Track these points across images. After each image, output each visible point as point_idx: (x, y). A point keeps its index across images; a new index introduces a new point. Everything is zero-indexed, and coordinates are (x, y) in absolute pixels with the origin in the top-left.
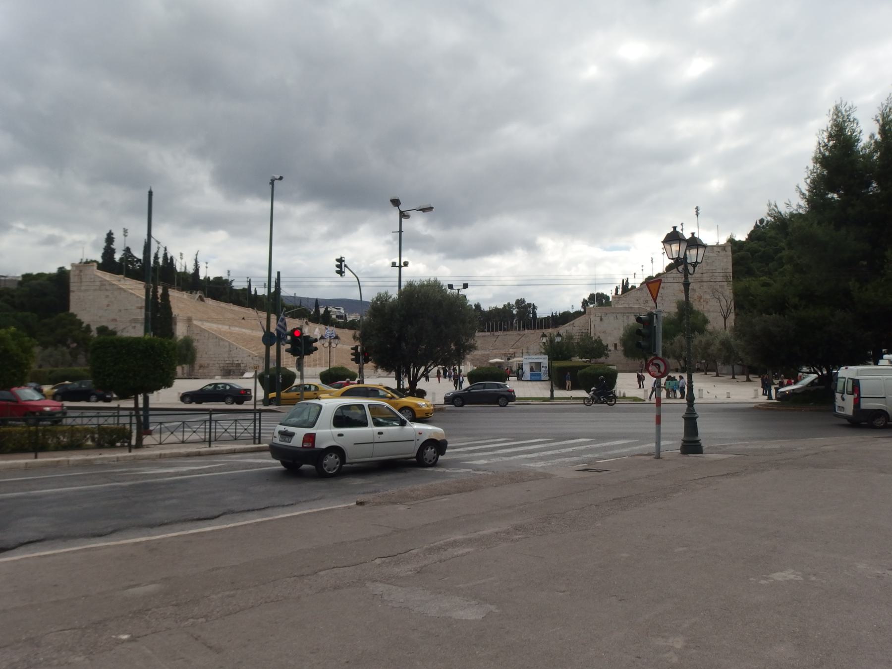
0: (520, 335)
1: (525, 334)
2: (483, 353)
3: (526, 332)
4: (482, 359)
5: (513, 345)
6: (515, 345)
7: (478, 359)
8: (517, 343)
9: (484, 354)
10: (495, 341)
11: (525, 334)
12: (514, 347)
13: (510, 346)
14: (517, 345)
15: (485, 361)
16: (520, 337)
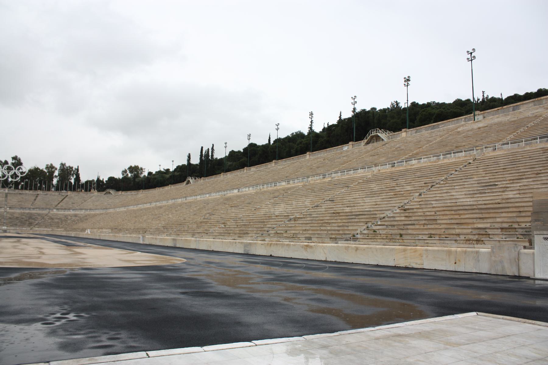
0: (63, 196)
1: (67, 195)
2: (23, 211)
3: (69, 193)
4: (22, 218)
5: (57, 205)
6: (59, 205)
7: (17, 218)
8: (61, 203)
9: (24, 213)
10: (35, 200)
11: (67, 195)
12: (57, 207)
13: (54, 206)
14: (62, 206)
15: (26, 220)
16: (63, 197)
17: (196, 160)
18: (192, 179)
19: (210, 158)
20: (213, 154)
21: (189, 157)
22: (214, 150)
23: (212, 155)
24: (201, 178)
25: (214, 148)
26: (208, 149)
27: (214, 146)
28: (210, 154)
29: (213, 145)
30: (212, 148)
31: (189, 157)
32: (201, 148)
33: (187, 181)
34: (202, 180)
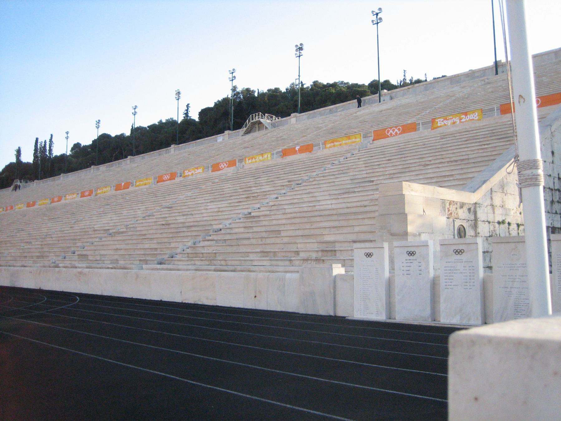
17: (28, 157)
18: (21, 182)
19: (47, 153)
20: (52, 147)
21: (19, 152)
22: (52, 142)
23: (50, 150)
24: (33, 181)
25: (53, 140)
26: (45, 141)
27: (53, 137)
28: (48, 148)
29: (52, 135)
30: (50, 140)
31: (19, 152)
32: (35, 139)
33: (14, 185)
34: (35, 184)
